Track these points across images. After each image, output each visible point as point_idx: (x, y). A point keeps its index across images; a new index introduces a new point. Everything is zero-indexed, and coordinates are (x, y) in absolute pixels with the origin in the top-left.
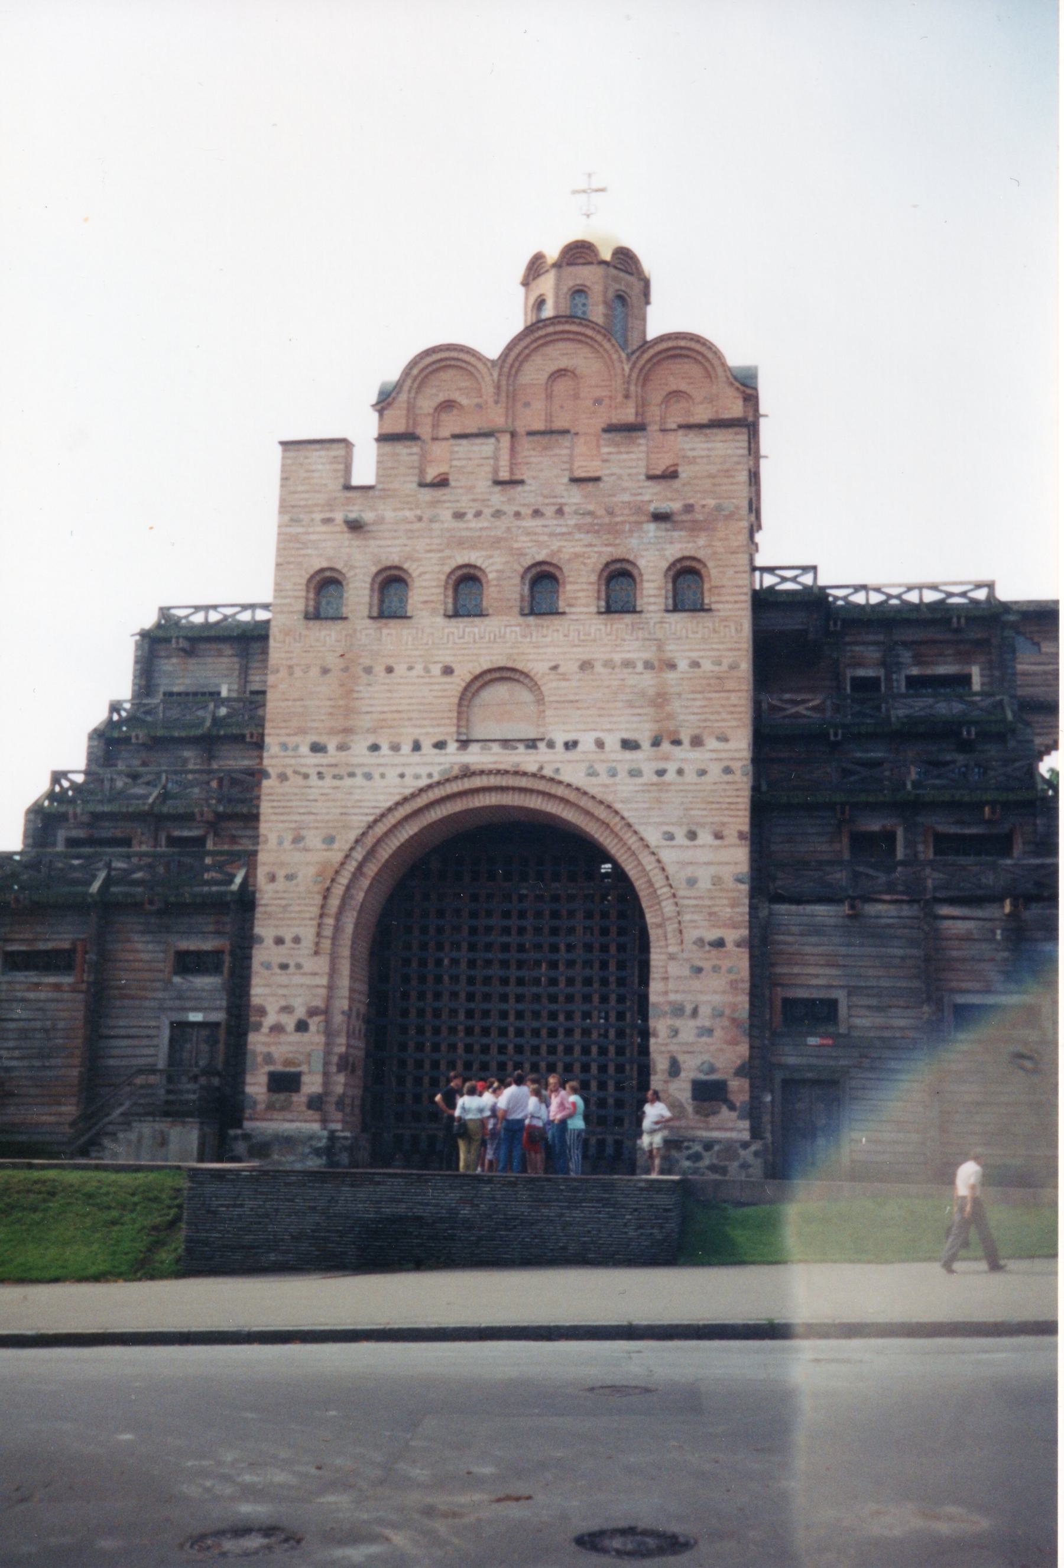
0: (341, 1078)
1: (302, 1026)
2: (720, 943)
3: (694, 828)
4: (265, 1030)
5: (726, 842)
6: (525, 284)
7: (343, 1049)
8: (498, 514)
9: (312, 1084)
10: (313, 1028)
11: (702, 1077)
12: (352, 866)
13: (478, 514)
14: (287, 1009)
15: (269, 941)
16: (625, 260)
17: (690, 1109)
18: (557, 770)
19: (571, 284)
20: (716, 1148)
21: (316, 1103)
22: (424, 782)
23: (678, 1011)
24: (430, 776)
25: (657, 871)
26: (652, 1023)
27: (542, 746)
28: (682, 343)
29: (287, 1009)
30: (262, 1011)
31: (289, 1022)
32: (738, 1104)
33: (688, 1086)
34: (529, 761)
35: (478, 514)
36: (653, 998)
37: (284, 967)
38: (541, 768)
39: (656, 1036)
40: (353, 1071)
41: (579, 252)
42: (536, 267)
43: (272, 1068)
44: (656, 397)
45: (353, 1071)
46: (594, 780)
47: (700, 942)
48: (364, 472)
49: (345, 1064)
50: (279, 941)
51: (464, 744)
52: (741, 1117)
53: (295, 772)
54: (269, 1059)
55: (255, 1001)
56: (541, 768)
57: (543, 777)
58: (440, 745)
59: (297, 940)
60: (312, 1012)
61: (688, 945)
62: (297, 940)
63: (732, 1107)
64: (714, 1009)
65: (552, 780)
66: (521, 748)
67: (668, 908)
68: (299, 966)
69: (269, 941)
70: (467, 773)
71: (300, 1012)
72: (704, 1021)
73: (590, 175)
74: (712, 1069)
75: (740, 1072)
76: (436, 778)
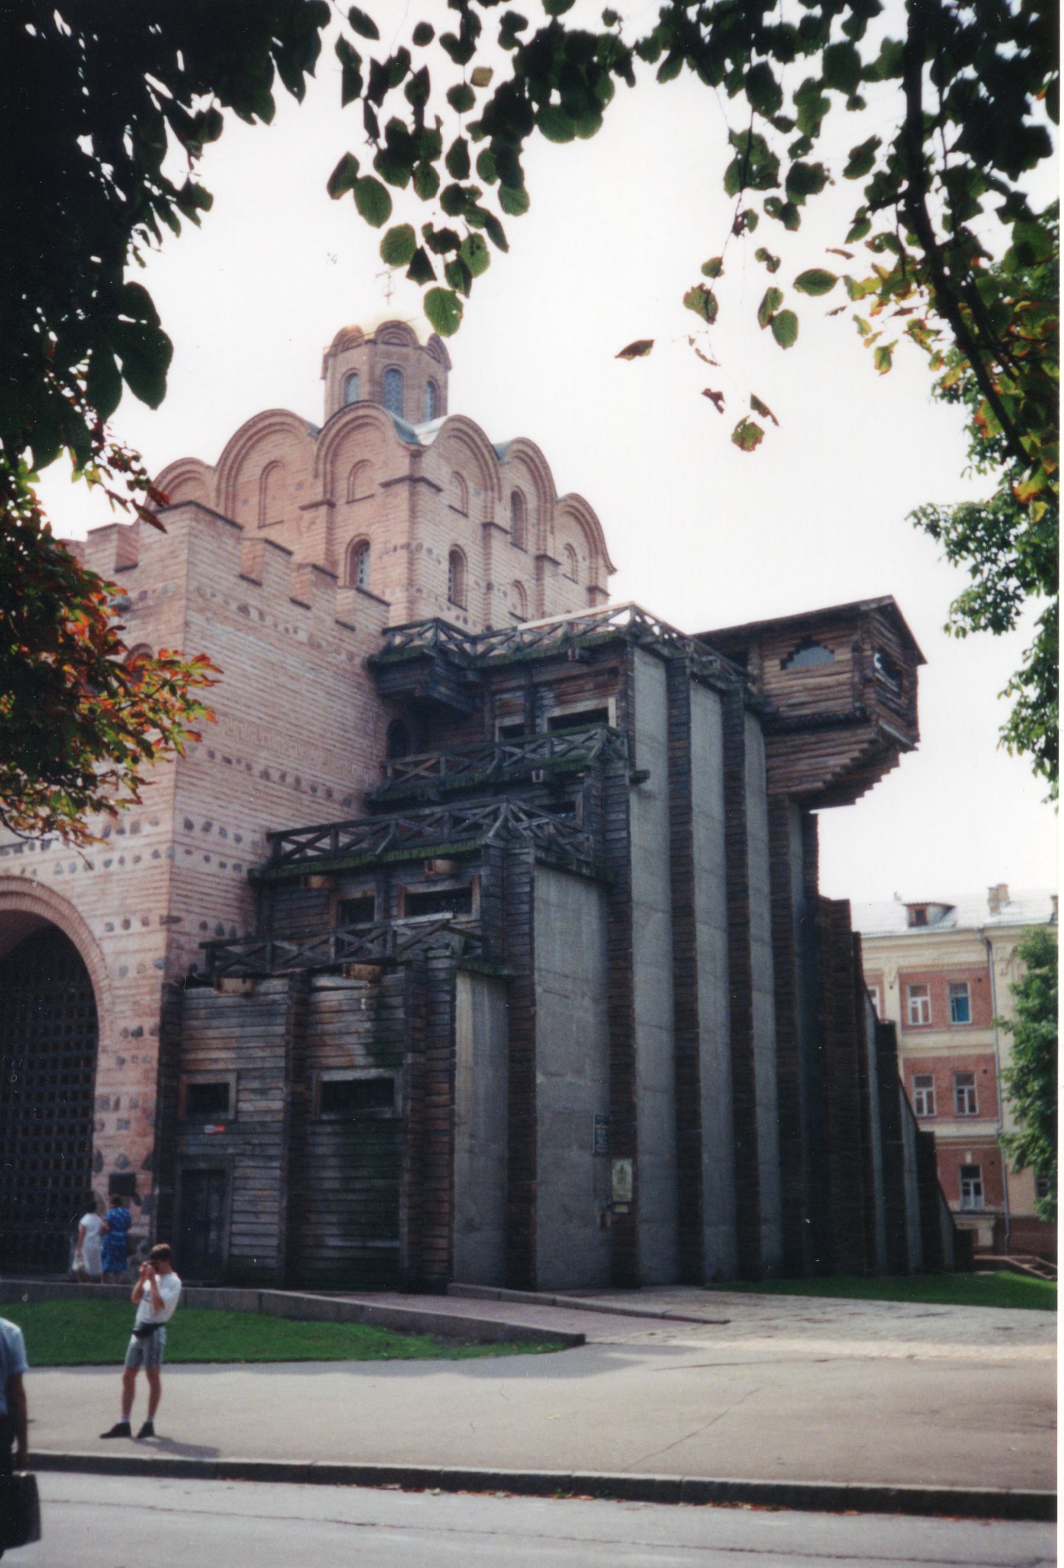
2: (139, 1033)
3: (128, 916)
5: (150, 928)
11: (119, 1171)
18: (34, 872)
19: (344, 370)
38: (23, 871)
44: (343, 468)
46: (59, 877)
47: (125, 1033)
52: (144, 1212)
56: (23, 871)
63: (138, 1202)
64: (131, 1100)
66: (11, 851)
72: (123, 1113)
75: (147, 1165)
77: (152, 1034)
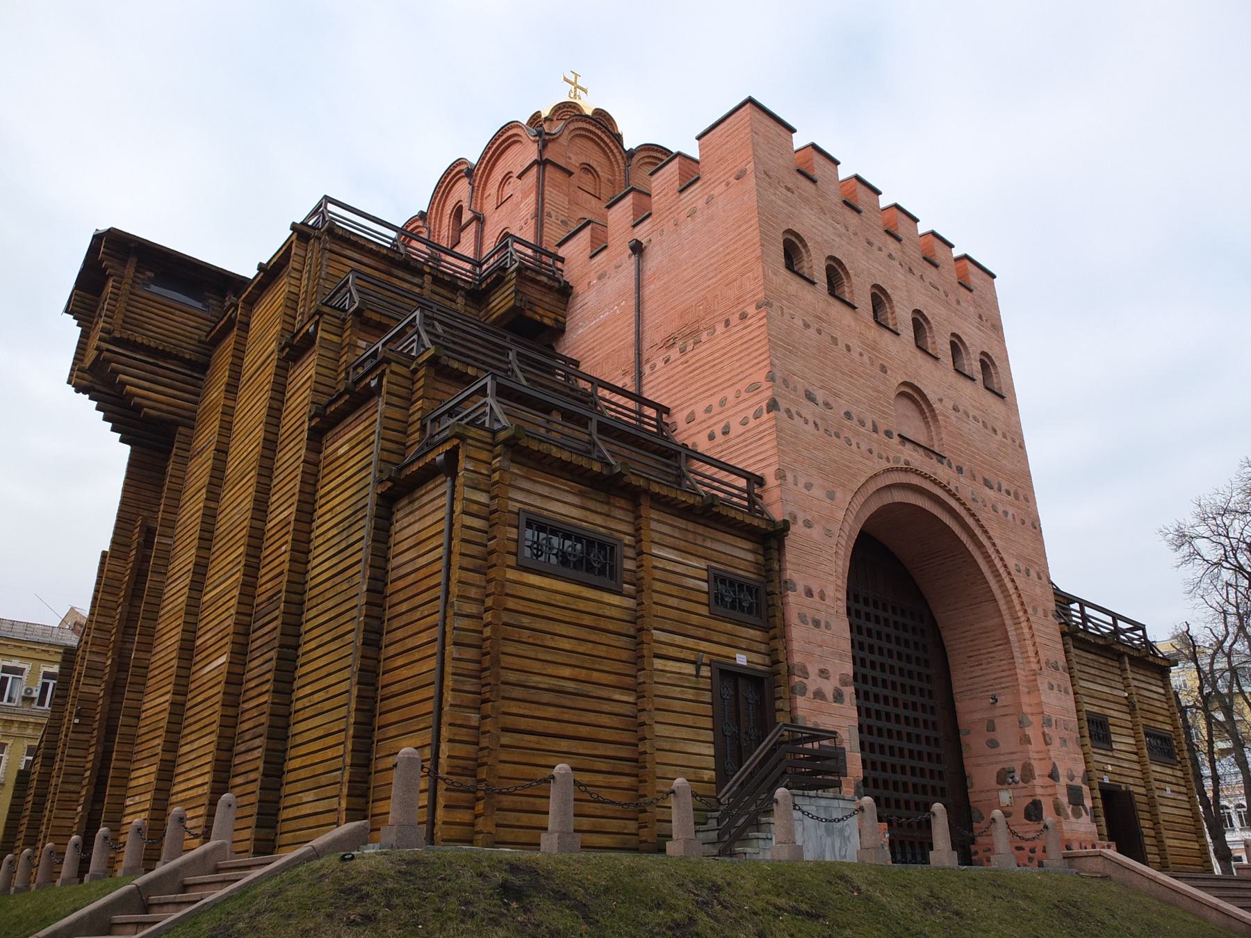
1: (838, 697)
4: (810, 694)
10: (847, 699)
14: (823, 673)
15: (800, 589)
17: (1069, 811)
22: (885, 465)
23: (1047, 722)
27: (945, 462)
29: (823, 673)
31: (828, 687)
33: (1065, 791)
34: (943, 473)
37: (817, 623)
50: (809, 593)
55: (797, 659)
57: (949, 491)
59: (822, 596)
61: (1043, 665)
65: (954, 495)
68: (828, 626)
69: (800, 589)
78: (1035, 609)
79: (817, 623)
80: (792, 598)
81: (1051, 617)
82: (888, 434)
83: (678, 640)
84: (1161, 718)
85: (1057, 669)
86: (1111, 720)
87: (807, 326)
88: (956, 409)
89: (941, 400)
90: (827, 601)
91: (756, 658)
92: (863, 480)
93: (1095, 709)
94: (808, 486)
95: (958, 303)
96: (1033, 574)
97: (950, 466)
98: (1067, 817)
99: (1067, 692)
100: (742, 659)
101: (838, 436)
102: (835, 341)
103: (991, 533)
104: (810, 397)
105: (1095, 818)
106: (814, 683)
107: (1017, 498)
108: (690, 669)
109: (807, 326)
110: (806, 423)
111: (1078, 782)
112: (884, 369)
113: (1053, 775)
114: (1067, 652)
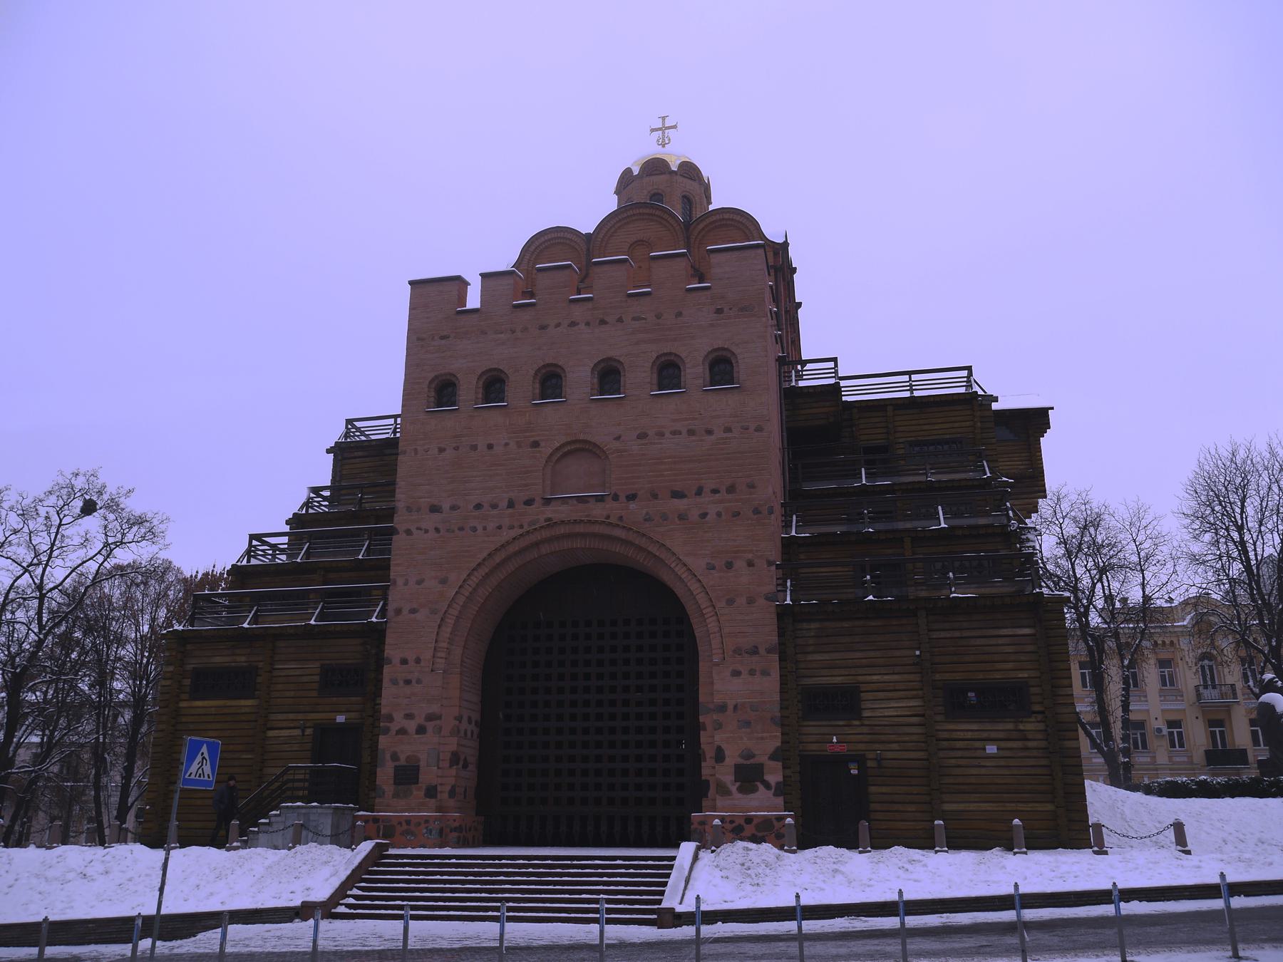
0: (453, 771)
1: (421, 730)
2: (754, 651)
6: (618, 192)
7: (454, 748)
8: (573, 324)
9: (429, 775)
10: (430, 730)
11: (741, 761)
12: (461, 600)
13: (558, 325)
15: (396, 661)
16: (690, 171)
17: (734, 789)
20: (755, 822)
21: (431, 792)
22: (517, 532)
23: (722, 708)
24: (521, 527)
25: (703, 594)
26: (702, 719)
28: (726, 216)
29: (409, 716)
30: (390, 718)
31: (411, 726)
32: (773, 784)
34: (598, 511)
35: (558, 325)
36: (701, 699)
37: (408, 682)
38: (608, 517)
39: (705, 729)
40: (465, 766)
41: (655, 167)
42: (626, 180)
43: (397, 764)
45: (465, 766)
47: (738, 651)
48: (473, 300)
49: (455, 759)
50: (404, 662)
51: (548, 501)
53: (418, 528)
54: (395, 757)
55: (384, 711)
58: (529, 502)
59: (418, 661)
60: (431, 717)
62: (418, 661)
63: (768, 786)
67: (712, 625)
69: (396, 661)
70: (551, 524)
71: (420, 720)
73: (664, 118)
74: (750, 756)
75: (773, 757)
76: (526, 528)
77: (769, 651)
78: (730, 602)
79: (408, 682)
80: (386, 669)
81: (762, 602)
82: (529, 502)
83: (291, 716)
84: (1010, 665)
85: (754, 651)
86: (863, 687)
87: (441, 450)
88: (643, 436)
89: (618, 438)
90: (422, 664)
91: (353, 715)
92: (485, 554)
93: (838, 680)
94: (419, 582)
95: (679, 314)
96: (740, 564)
97: (616, 498)
98: (728, 793)
99: (765, 673)
100: (341, 719)
101: (461, 529)
102: (474, 448)
103: (668, 544)
104: (435, 509)
105: (780, 790)
106: (399, 721)
107: (731, 489)
108: (297, 732)
109: (441, 450)
110: (426, 531)
111: (763, 759)
112: (536, 444)
113: (720, 756)
114: (781, 633)
